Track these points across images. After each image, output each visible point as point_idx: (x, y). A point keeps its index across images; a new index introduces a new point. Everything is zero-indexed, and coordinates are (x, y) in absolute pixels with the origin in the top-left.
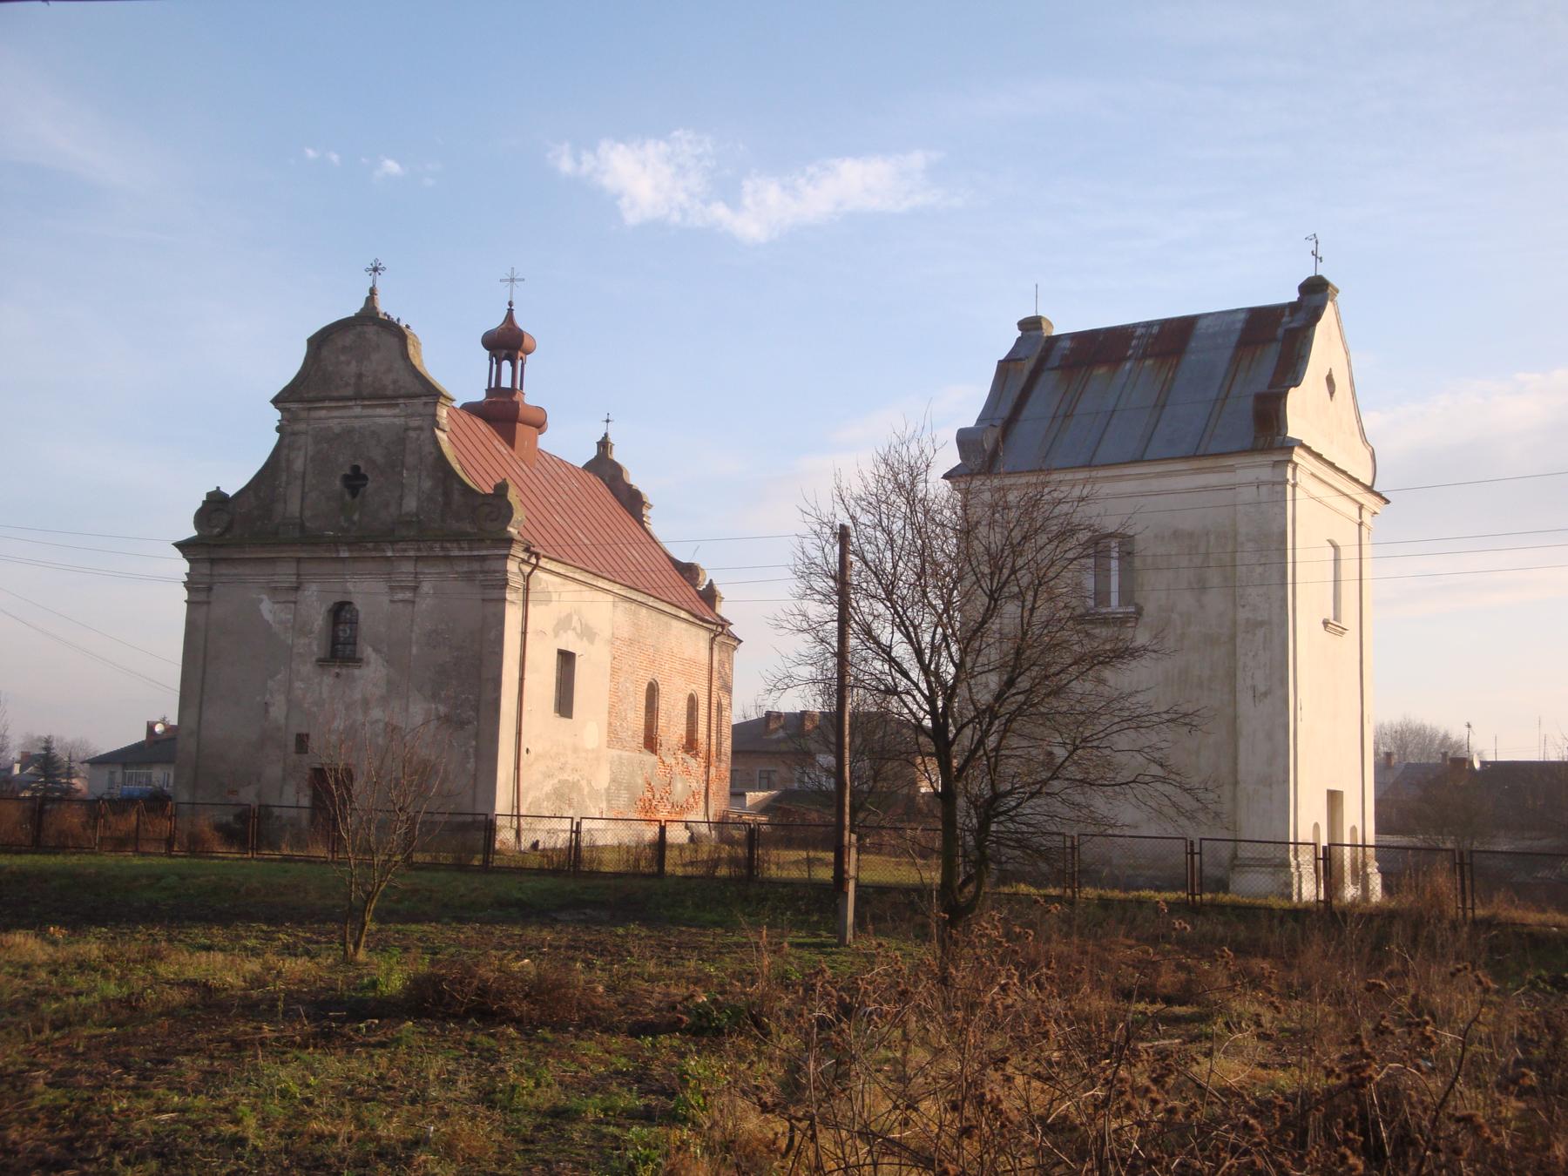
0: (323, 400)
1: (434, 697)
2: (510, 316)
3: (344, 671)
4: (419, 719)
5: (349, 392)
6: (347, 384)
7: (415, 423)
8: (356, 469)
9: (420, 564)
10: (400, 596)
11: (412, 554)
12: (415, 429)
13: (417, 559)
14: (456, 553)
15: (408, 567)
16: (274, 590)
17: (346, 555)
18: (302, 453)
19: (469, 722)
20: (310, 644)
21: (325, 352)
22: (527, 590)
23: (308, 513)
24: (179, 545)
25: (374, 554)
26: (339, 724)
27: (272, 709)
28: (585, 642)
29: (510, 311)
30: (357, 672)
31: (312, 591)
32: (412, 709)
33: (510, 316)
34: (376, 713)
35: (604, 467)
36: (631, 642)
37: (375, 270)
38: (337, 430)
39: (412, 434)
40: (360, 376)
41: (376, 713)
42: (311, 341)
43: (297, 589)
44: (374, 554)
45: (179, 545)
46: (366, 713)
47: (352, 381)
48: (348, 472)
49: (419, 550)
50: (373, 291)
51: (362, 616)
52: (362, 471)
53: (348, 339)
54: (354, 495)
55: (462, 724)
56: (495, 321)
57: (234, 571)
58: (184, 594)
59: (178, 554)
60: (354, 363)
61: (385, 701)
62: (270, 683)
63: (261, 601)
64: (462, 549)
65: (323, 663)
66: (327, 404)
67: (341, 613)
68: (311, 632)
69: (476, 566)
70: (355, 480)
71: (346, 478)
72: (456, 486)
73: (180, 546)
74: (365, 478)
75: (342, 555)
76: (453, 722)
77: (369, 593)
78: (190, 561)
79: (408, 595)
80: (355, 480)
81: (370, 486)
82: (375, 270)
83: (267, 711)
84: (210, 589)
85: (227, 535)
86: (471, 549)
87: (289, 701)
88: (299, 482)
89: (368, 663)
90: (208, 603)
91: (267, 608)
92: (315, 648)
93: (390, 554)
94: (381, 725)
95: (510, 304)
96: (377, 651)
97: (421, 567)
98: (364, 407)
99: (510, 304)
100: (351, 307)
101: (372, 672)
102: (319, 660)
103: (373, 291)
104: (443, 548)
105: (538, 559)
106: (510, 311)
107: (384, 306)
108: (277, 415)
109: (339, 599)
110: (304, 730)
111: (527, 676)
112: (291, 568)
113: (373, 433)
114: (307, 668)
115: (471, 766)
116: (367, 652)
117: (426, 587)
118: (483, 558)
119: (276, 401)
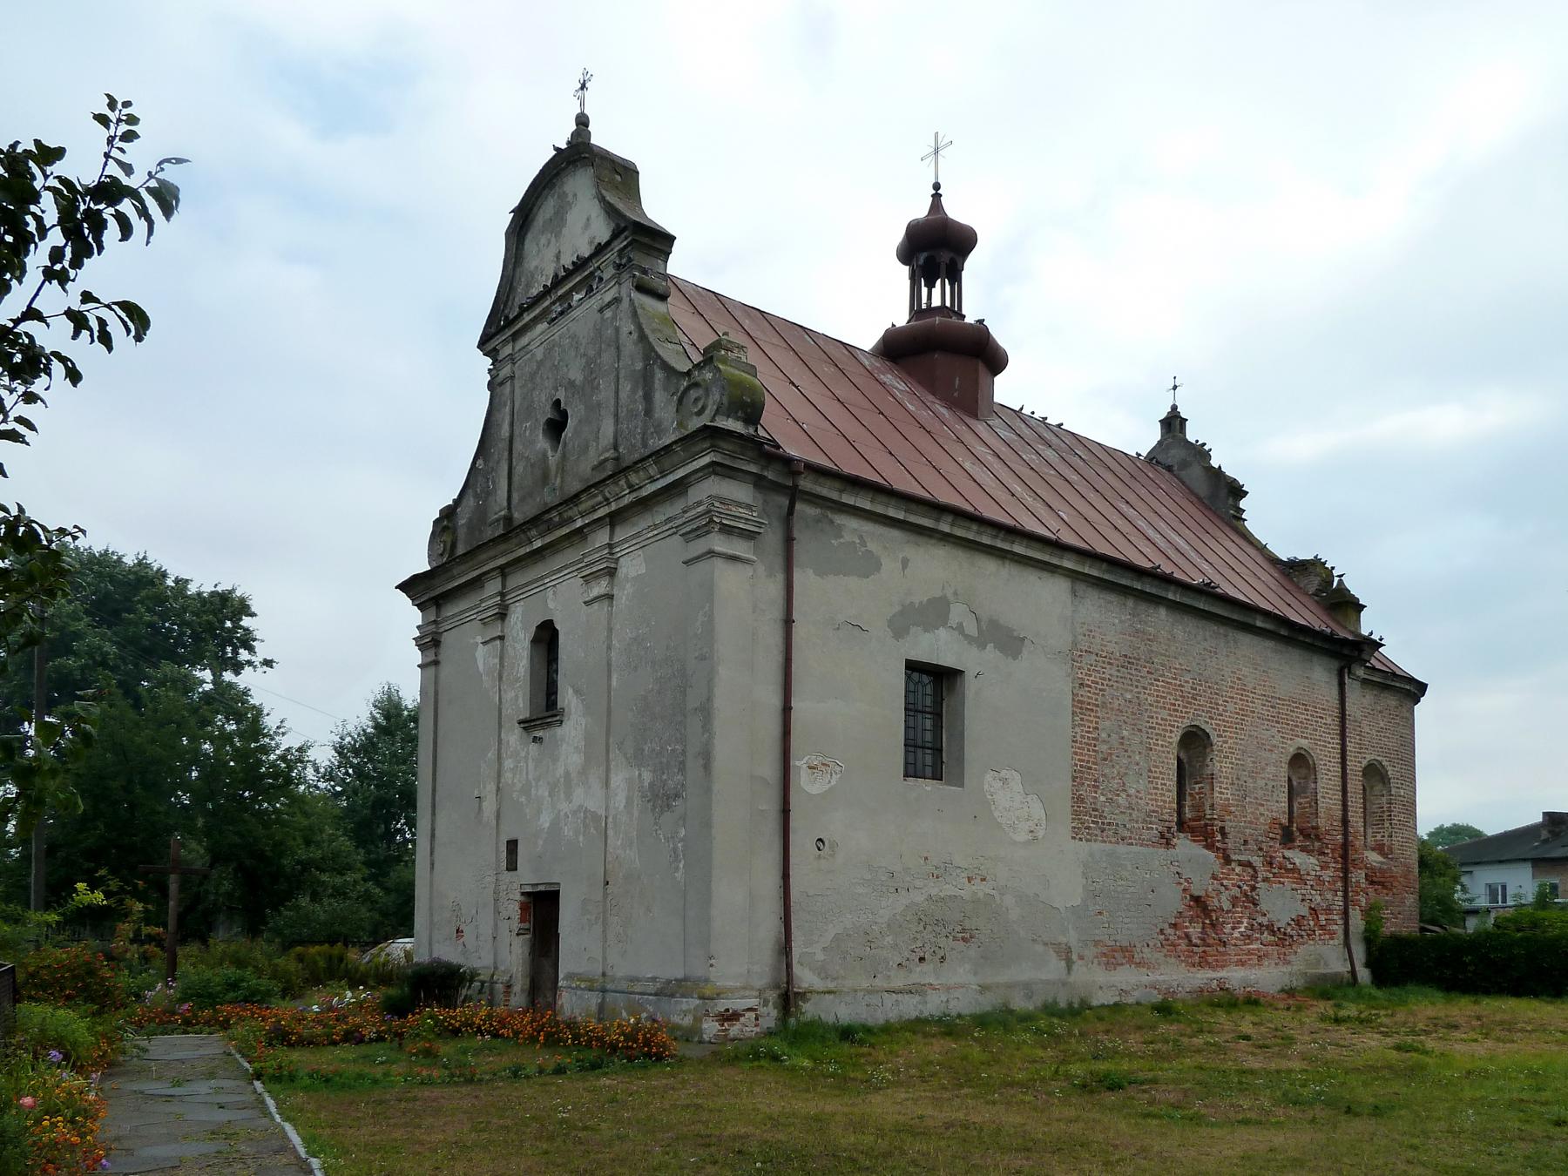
11: (601, 513)
26: (545, 821)
28: (991, 653)
30: (559, 731)
35: (1176, 445)
36: (1128, 661)
41: (579, 794)
45: (403, 587)
58: (417, 656)
68: (517, 680)
69: (673, 509)
96: (577, 692)
104: (633, 489)
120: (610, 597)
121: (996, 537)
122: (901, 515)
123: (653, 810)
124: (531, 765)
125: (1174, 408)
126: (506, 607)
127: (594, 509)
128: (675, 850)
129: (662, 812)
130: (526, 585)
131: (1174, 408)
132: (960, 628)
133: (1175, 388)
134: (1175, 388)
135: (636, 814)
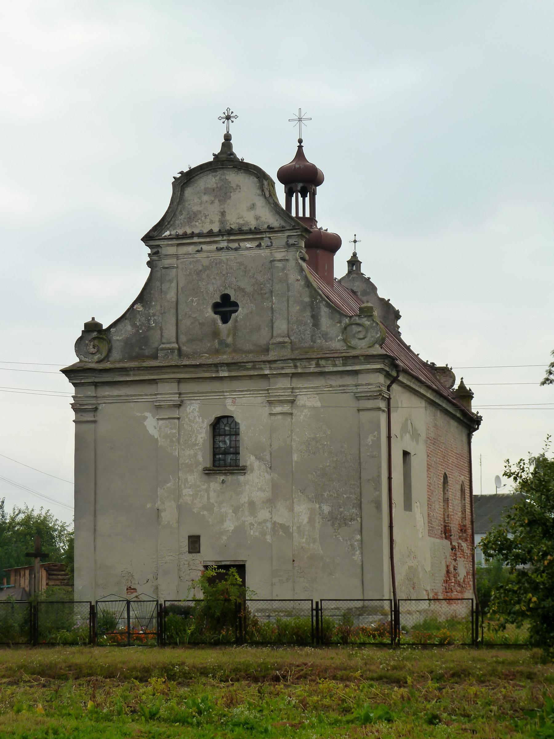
1: (318, 498)
2: (300, 154)
3: (230, 478)
4: (304, 519)
6: (212, 222)
8: (226, 298)
9: (295, 380)
10: (278, 409)
13: (294, 375)
14: (331, 369)
15: (285, 383)
17: (226, 374)
18: (174, 284)
19: (351, 520)
20: (196, 455)
21: (189, 192)
22: (389, 400)
24: (64, 371)
26: (230, 526)
27: (163, 514)
29: (300, 147)
30: (242, 478)
31: (193, 409)
32: (297, 508)
33: (300, 154)
34: (263, 514)
37: (228, 118)
38: (205, 262)
40: (223, 214)
41: (263, 514)
43: (179, 406)
44: (252, 373)
45: (64, 371)
47: (217, 218)
48: (219, 300)
49: (296, 367)
50: (228, 138)
51: (243, 428)
52: (232, 299)
54: (225, 320)
55: (345, 521)
56: (287, 158)
59: (64, 378)
61: (271, 502)
62: (160, 491)
64: (335, 365)
65: (209, 472)
66: (196, 240)
67: (223, 428)
69: (349, 380)
70: (225, 307)
71: (216, 307)
72: (324, 310)
73: (67, 372)
74: (236, 305)
75: (222, 374)
76: (337, 520)
77: (247, 407)
78: (75, 385)
79: (286, 408)
80: (225, 307)
81: (241, 312)
82: (228, 118)
83: (158, 516)
84: (96, 409)
85: (104, 363)
86: (344, 365)
88: (173, 311)
89: (252, 471)
90: (95, 422)
91: (151, 425)
92: (201, 459)
93: (267, 372)
94: (269, 525)
95: (300, 141)
97: (297, 383)
99: (300, 141)
101: (256, 481)
102: (205, 469)
103: (228, 138)
104: (318, 365)
105: (398, 372)
106: (300, 147)
107: (242, 152)
110: (195, 532)
111: (393, 476)
112: (172, 388)
113: (241, 264)
114: (194, 477)
115: (357, 557)
116: (247, 458)
117: (302, 400)
120: (291, 414)
121: (421, 387)
122: (408, 383)
123: (333, 525)
125: (355, 255)
126: (182, 401)
127: (283, 368)
128: (352, 545)
129: (340, 526)
130: (198, 393)
131: (355, 255)
132: (409, 432)
133: (355, 241)
134: (355, 241)
135: (318, 526)
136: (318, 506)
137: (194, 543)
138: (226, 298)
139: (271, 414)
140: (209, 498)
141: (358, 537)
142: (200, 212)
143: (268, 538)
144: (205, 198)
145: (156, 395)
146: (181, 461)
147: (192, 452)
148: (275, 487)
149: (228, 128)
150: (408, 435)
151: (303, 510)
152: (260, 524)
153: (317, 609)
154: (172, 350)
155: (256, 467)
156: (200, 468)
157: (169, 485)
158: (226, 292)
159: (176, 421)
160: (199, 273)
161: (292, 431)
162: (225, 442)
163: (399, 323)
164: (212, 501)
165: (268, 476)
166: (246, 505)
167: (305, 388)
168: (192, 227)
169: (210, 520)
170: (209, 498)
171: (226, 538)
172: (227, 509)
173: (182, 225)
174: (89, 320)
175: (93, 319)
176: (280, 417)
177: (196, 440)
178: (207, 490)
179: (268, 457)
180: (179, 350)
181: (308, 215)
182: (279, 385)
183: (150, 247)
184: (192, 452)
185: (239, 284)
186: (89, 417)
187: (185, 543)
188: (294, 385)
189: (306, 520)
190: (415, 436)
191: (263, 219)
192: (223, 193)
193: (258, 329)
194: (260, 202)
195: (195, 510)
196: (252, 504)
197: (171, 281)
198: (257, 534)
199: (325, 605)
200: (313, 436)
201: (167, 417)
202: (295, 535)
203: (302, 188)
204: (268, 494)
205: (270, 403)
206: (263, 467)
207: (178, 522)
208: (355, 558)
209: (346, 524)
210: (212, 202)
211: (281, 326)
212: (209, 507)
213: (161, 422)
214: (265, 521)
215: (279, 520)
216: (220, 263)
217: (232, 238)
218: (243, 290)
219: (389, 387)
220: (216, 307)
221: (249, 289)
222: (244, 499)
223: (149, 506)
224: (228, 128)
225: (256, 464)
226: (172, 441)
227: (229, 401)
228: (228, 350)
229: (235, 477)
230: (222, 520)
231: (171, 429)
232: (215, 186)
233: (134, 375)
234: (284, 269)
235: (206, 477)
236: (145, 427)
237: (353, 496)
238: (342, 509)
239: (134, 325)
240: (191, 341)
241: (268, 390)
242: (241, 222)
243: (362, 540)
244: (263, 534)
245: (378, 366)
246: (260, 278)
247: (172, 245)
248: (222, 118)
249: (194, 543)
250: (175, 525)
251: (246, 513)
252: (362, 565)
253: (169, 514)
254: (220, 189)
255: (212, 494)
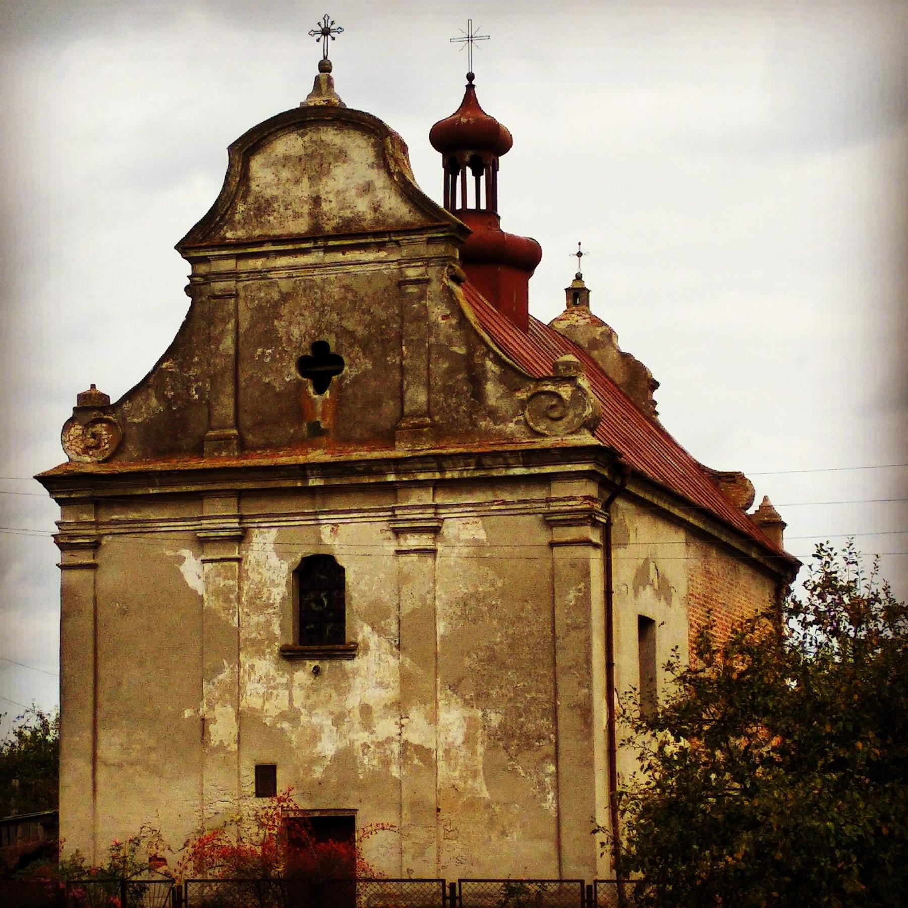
0: (260, 243)
1: (480, 698)
2: (470, 100)
3: (326, 666)
4: (457, 735)
5: (301, 226)
6: (297, 216)
7: (412, 273)
8: (320, 347)
10: (413, 541)
12: (416, 282)
15: (426, 497)
16: (202, 543)
17: (319, 482)
18: (230, 326)
19: (540, 738)
20: (268, 623)
21: (257, 165)
23: (247, 420)
25: (366, 480)
26: (328, 747)
27: (212, 728)
29: (470, 88)
30: (348, 665)
33: (470, 100)
34: (386, 727)
37: (326, 32)
39: (412, 289)
40: (317, 201)
42: (232, 149)
44: (366, 480)
46: (367, 726)
47: (306, 209)
50: (325, 66)
51: (349, 577)
52: (333, 349)
53: (289, 145)
55: (527, 741)
56: (448, 106)
57: (133, 515)
60: (305, 181)
61: (399, 707)
62: (207, 687)
63: (181, 560)
65: (290, 656)
78: (60, 502)
82: (326, 32)
84: (95, 546)
87: (239, 716)
90: (94, 567)
91: (193, 571)
92: (278, 631)
93: (392, 478)
94: (396, 747)
95: (470, 77)
98: (328, 250)
99: (470, 77)
100: (293, 94)
101: (373, 670)
103: (325, 66)
106: (470, 88)
108: (186, 268)
109: (310, 551)
113: (347, 288)
115: (550, 802)
117: (453, 527)
118: (545, 480)
119: (184, 247)
120: (434, 552)
124: (298, 694)
125: (578, 277)
126: (245, 530)
128: (540, 783)
129: (519, 750)
131: (578, 277)
133: (579, 254)
134: (579, 254)
135: (480, 749)
136: (480, 714)
137: (266, 778)
138: (320, 347)
139: (398, 552)
140: (291, 700)
141: (552, 768)
142: (275, 198)
143: (395, 771)
144: (285, 174)
145: (200, 518)
146: (243, 634)
147: (262, 619)
148: (405, 678)
149: (326, 50)
150: (648, 588)
151: (453, 719)
152: (380, 744)
153: (453, 896)
154: (227, 438)
155: (372, 646)
156: (277, 646)
157: (221, 677)
158: (323, 338)
159: (236, 564)
160: (276, 305)
161: (435, 582)
162: (319, 602)
163: (656, 395)
164: (296, 705)
165: (393, 662)
166: (357, 712)
167: (458, 506)
168: (261, 225)
169: (293, 737)
170: (291, 700)
171: (321, 770)
172: (322, 719)
173: (246, 222)
174: (86, 388)
175: (93, 386)
176: (414, 557)
177: (269, 598)
178: (288, 686)
179: (394, 628)
180: (241, 440)
181: (483, 206)
182: (413, 502)
183: (193, 261)
184: (262, 619)
185: (344, 323)
186: (84, 558)
187: (250, 777)
188: (439, 501)
189: (460, 740)
190: (664, 590)
191: (385, 209)
192: (316, 164)
193: (377, 403)
194: (379, 179)
195: (268, 722)
196: (366, 710)
197: (225, 321)
198: (375, 762)
199: (467, 888)
200: (471, 590)
201: (219, 557)
202: (441, 764)
203: (472, 158)
204: (391, 694)
205: (397, 532)
206: (385, 645)
207: (238, 742)
208: (546, 805)
209: (530, 746)
210: (297, 181)
211: (418, 397)
212: (291, 716)
213: (208, 566)
214: (389, 740)
215: (414, 738)
216: (311, 287)
217: (331, 243)
218: (352, 334)
219: (607, 506)
220: (303, 365)
221: (360, 331)
222: (353, 701)
223: (187, 713)
224: (326, 50)
225: (374, 640)
226: (227, 600)
227: (326, 531)
228: (324, 440)
229: (336, 664)
230: (315, 737)
231: (226, 578)
232: (302, 152)
233: (162, 485)
234: (422, 296)
235: (285, 664)
236: (180, 575)
237: (542, 696)
238: (522, 719)
239: (162, 398)
240: (259, 424)
241: (393, 510)
242: (347, 214)
243: (557, 774)
244: (386, 762)
245: (586, 467)
246: (382, 314)
247: (227, 257)
248: (316, 32)
249: (266, 778)
250: (234, 747)
251: (357, 726)
252: (558, 818)
253: (223, 729)
254: (311, 157)
255: (298, 694)
